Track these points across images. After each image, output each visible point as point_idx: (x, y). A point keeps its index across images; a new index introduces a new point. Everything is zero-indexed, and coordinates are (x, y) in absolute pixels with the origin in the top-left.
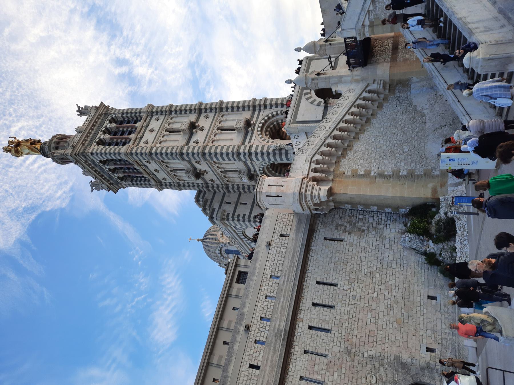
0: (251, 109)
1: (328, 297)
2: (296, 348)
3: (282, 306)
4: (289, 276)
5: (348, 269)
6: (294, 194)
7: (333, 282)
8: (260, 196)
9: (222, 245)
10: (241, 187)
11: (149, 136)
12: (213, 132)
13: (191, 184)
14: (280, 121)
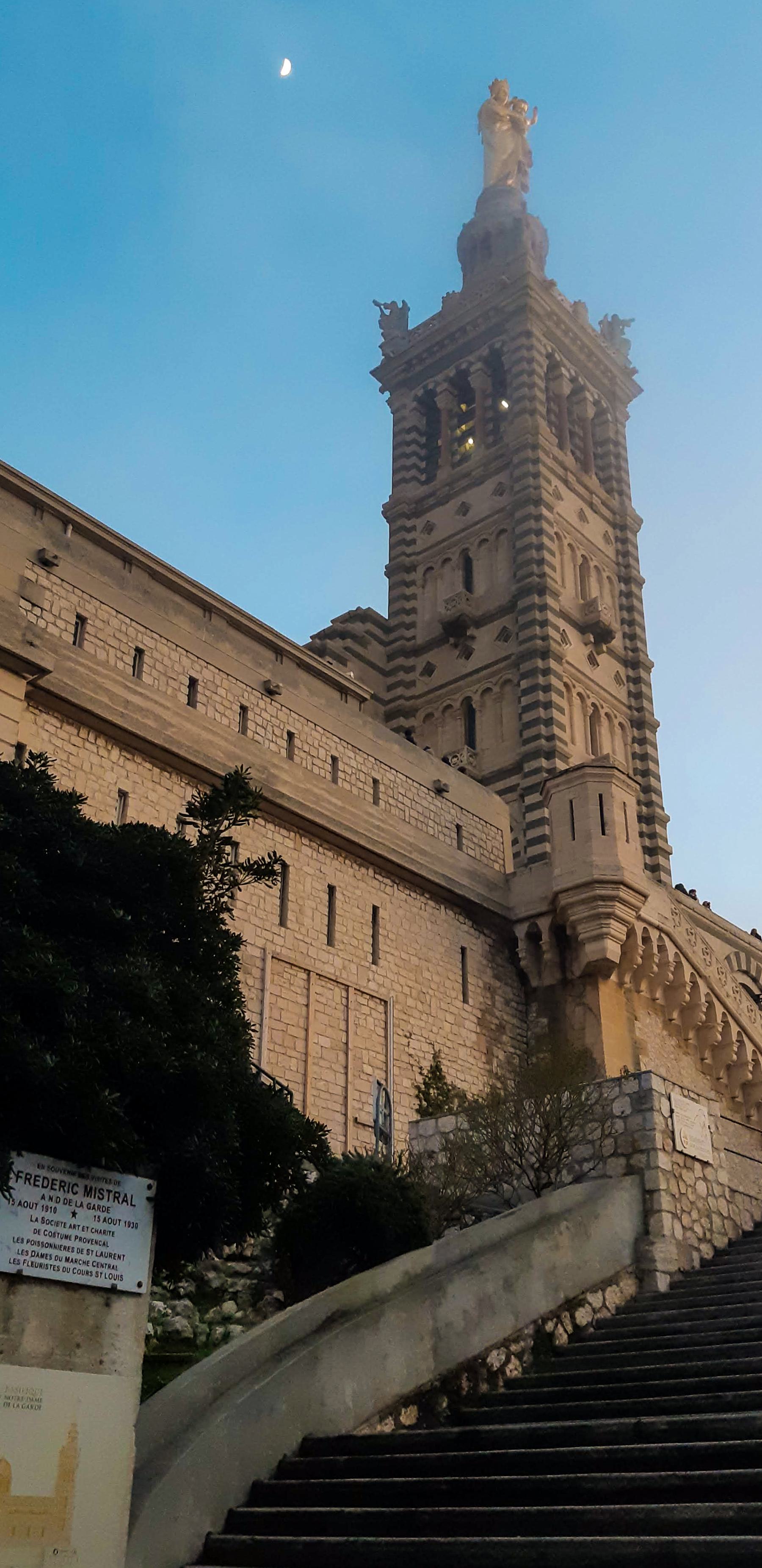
1: (350, 933)
4: (383, 830)
5: (410, 1002)
6: (619, 868)
7: (381, 954)
8: (601, 776)
12: (588, 692)
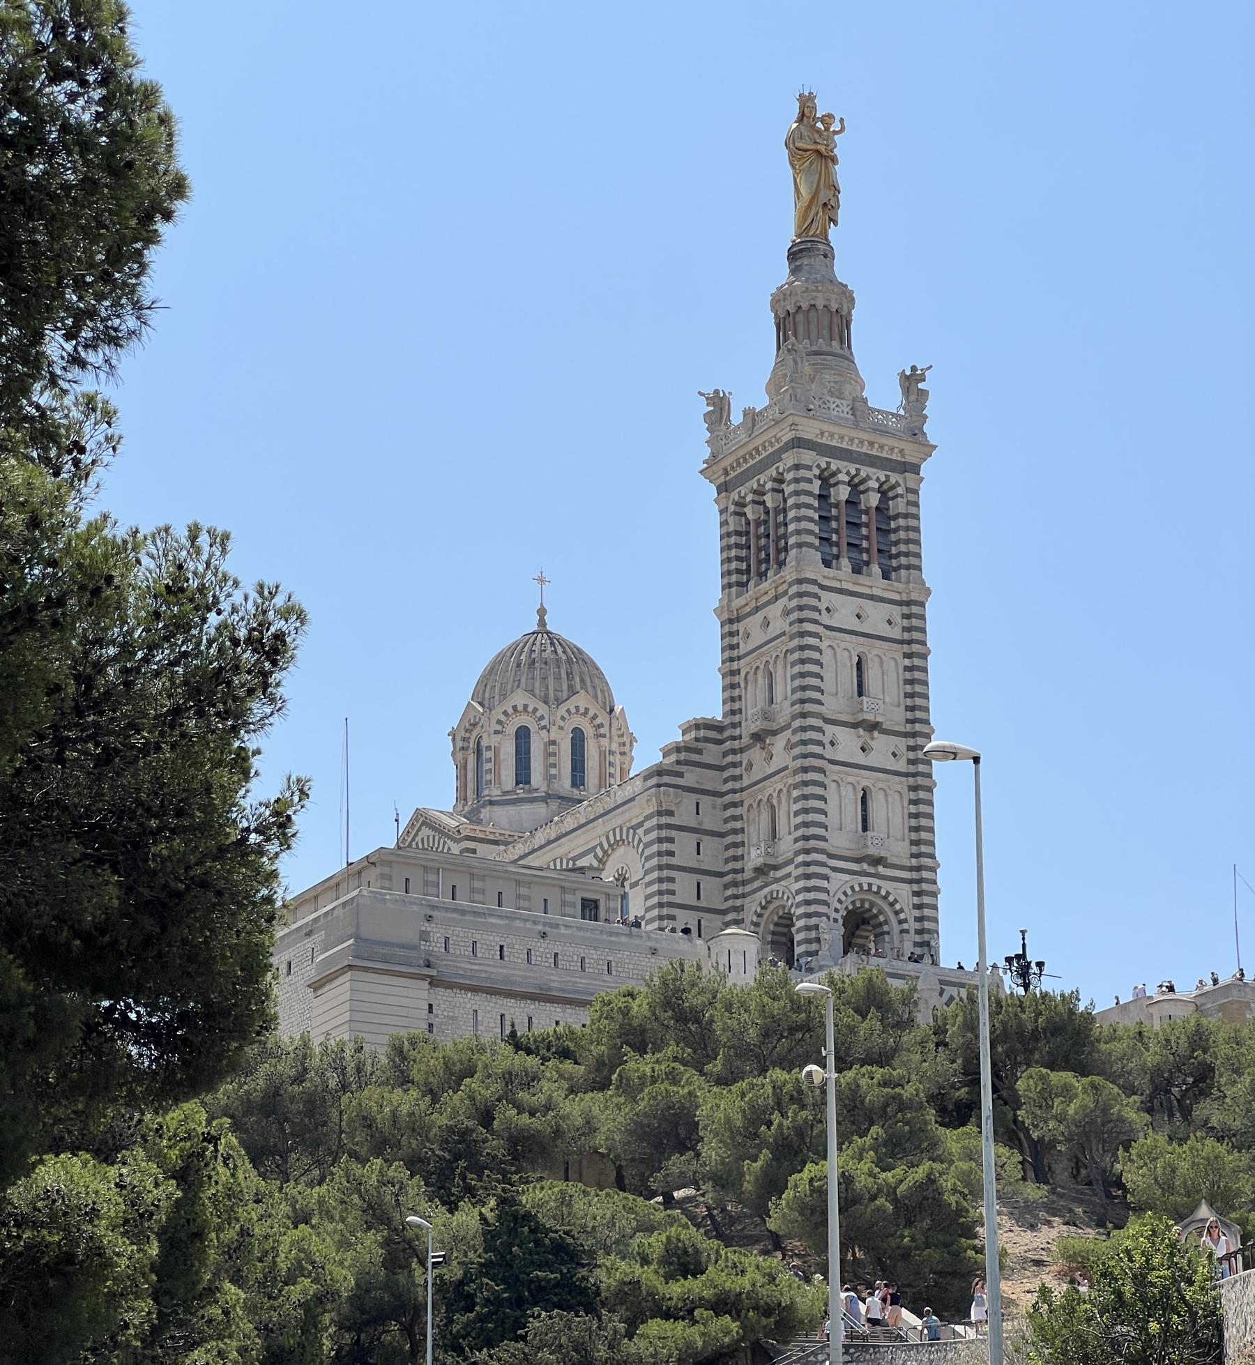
0: (914, 862)
2: (532, 1007)
3: (576, 982)
9: (542, 718)
10: (738, 838)
11: (844, 611)
13: (737, 706)
14: (885, 928)
